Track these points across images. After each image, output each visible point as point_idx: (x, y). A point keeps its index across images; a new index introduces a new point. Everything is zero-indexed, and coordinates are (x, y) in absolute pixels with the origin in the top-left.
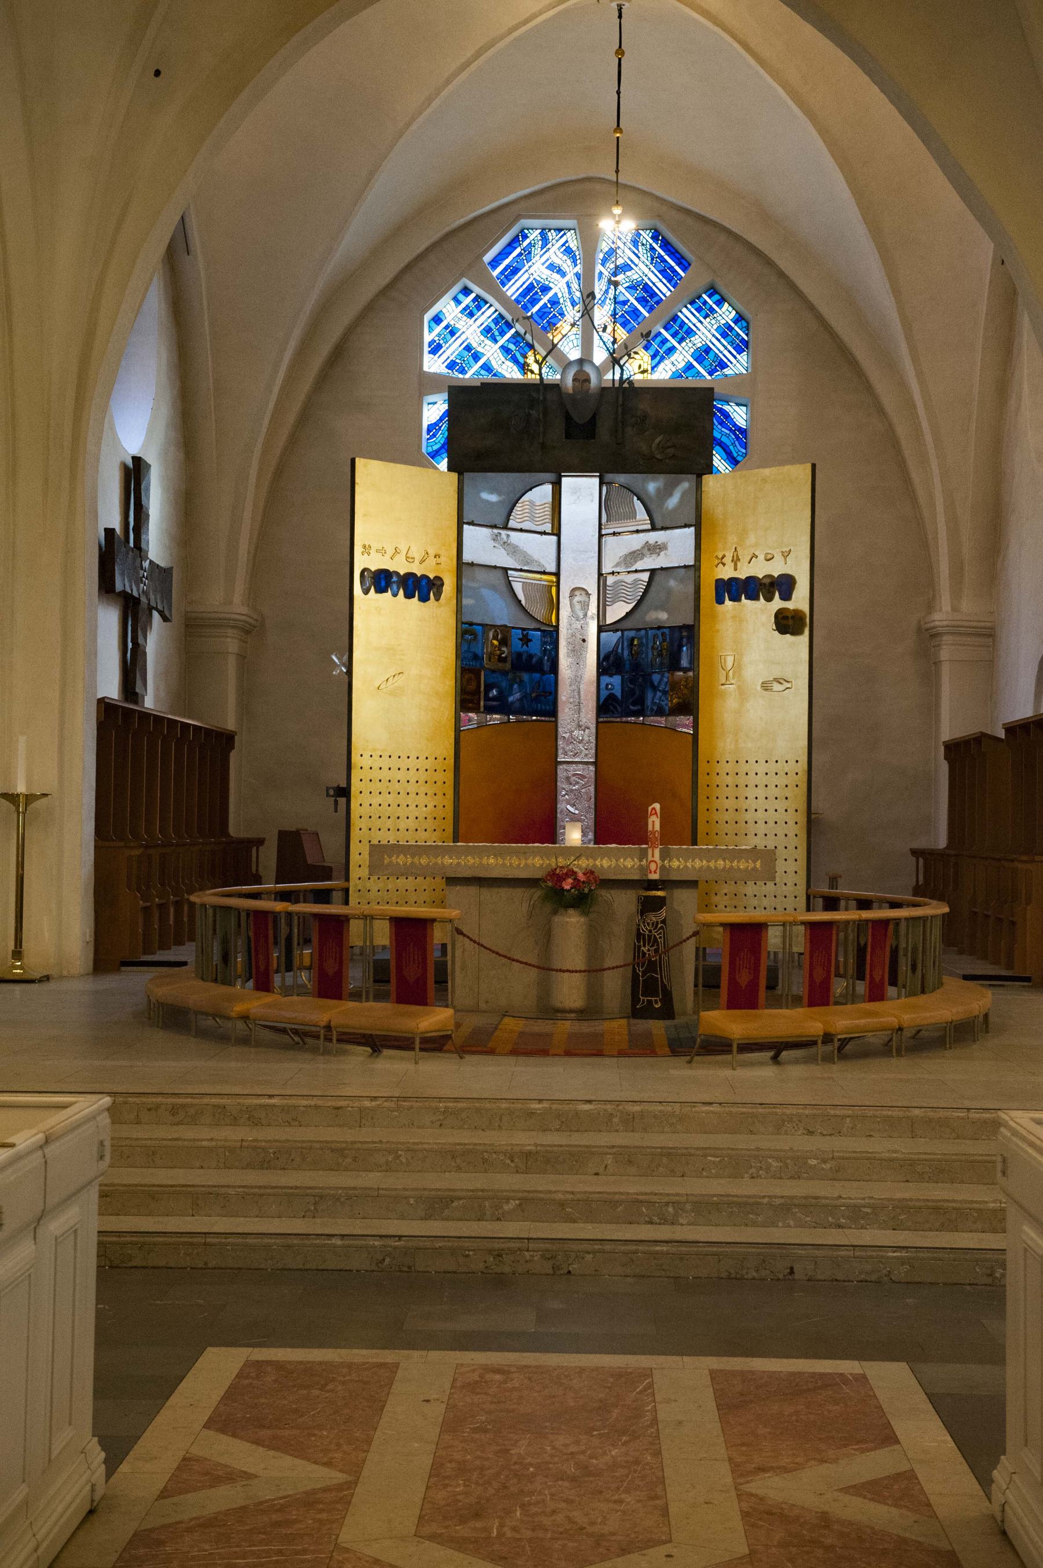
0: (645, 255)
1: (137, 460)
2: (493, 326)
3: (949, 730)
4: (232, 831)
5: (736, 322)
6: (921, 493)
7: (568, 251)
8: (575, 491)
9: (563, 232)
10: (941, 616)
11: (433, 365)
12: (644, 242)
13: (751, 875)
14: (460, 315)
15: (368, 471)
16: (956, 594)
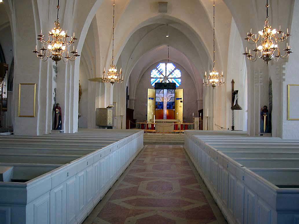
3: (198, 110)
4: (134, 119)
10: (198, 99)
11: (152, 76)
16: (199, 97)
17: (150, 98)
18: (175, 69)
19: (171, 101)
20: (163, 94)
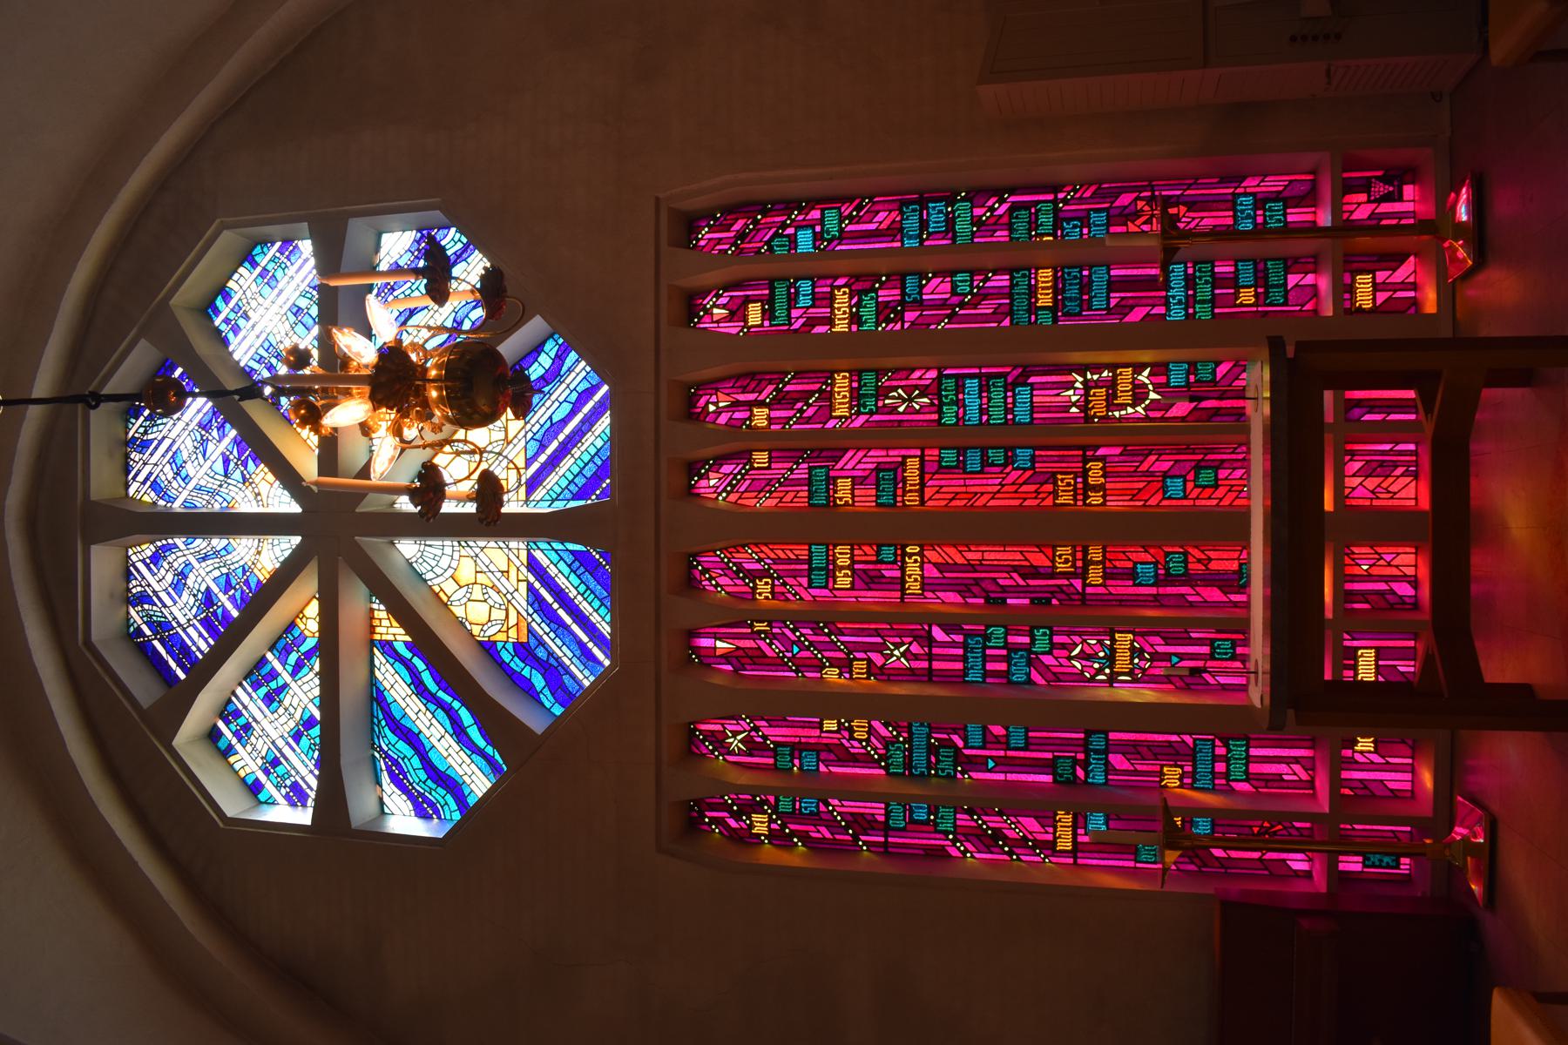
0: (161, 427)
2: (263, 691)
5: (254, 264)
7: (156, 559)
9: (131, 568)
12: (142, 430)
14: (249, 748)
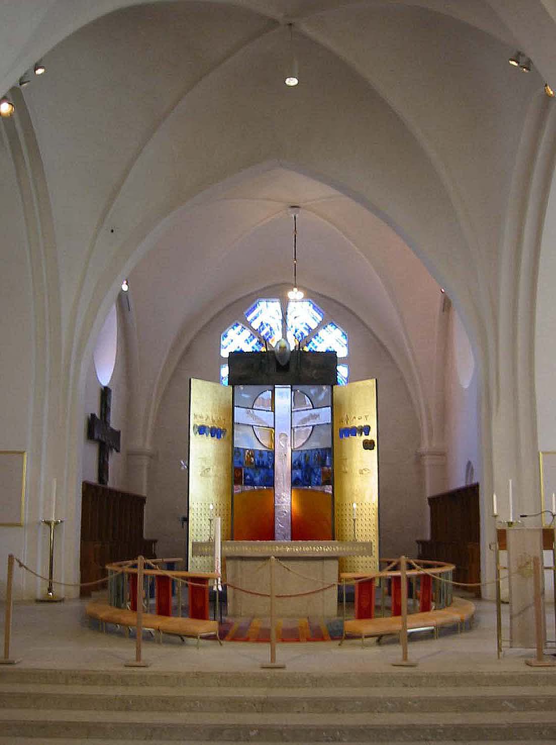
1: (106, 388)
4: (145, 536)
6: (415, 401)
8: (281, 394)
10: (425, 447)
13: (362, 554)
15: (196, 384)
16: (430, 437)
17: (202, 430)
18: (322, 325)
19: (314, 445)
20: (273, 410)
